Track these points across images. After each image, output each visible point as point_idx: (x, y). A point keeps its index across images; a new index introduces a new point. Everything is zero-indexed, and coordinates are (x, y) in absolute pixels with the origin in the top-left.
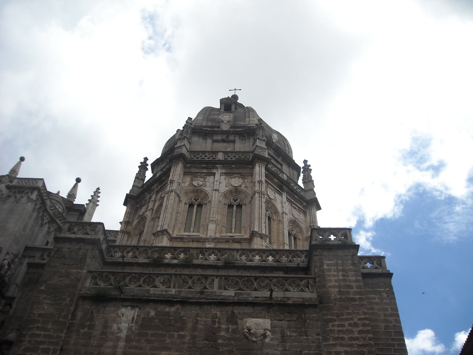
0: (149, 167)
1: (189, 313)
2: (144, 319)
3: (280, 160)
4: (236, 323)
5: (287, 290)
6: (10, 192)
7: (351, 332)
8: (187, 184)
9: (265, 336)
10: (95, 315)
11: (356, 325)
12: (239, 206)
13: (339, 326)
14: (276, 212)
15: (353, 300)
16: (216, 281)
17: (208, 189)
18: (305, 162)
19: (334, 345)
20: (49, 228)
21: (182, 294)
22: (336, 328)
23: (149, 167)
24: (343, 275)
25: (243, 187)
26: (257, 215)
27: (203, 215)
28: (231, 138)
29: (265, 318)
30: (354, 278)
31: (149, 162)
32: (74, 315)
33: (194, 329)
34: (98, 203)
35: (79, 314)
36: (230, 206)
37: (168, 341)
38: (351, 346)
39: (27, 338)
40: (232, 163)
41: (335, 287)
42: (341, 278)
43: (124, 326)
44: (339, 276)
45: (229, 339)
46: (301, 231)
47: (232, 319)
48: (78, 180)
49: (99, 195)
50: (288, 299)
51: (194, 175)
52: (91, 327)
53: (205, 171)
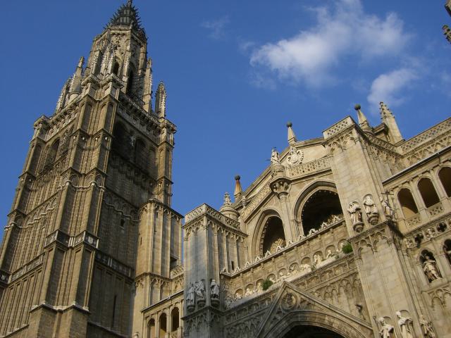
6: (330, 145)
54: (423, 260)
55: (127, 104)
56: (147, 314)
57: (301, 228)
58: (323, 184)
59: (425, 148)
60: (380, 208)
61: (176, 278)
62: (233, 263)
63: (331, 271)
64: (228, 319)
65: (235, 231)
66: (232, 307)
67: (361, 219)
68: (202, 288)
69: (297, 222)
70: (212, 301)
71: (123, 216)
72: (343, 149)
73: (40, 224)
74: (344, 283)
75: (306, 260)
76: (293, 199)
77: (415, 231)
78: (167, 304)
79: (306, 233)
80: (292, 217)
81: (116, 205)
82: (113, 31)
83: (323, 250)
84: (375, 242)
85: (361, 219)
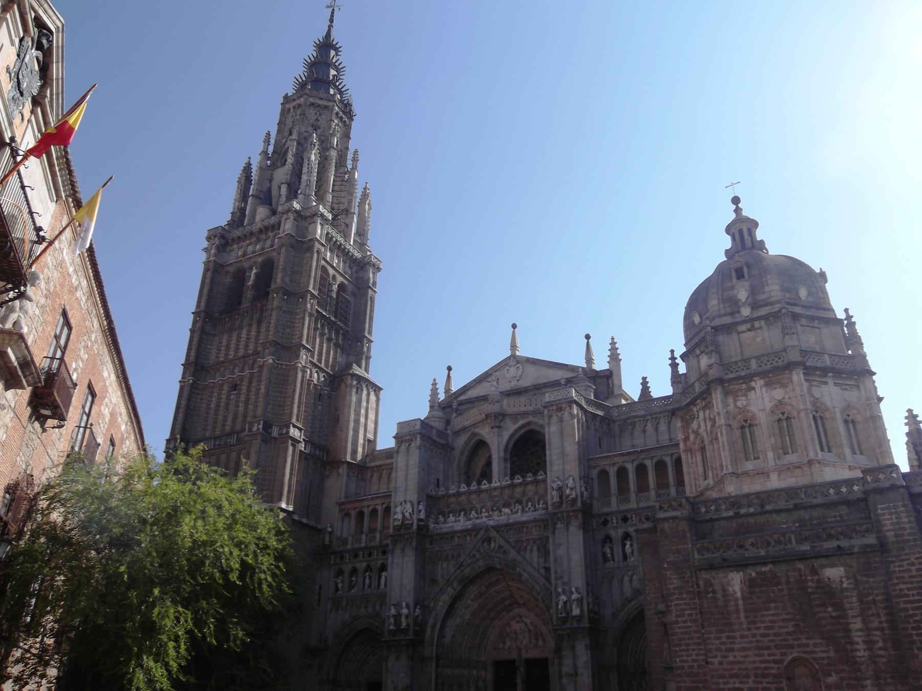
0: (679, 361)
2: (749, 580)
4: (817, 574)
5: (851, 538)
7: (910, 571)
8: (732, 407)
9: (842, 582)
10: (713, 581)
11: (913, 564)
12: (788, 418)
13: (900, 566)
15: (908, 541)
17: (754, 409)
18: (846, 310)
19: (897, 584)
20: (595, 425)
22: (897, 569)
23: (679, 361)
24: (897, 518)
25: (786, 400)
27: (758, 440)
28: (757, 324)
29: (837, 566)
30: (906, 520)
31: (677, 354)
33: (788, 583)
34: (620, 357)
35: (701, 583)
36: (779, 420)
37: (772, 595)
38: (911, 583)
39: (673, 608)
40: (769, 372)
41: (890, 530)
42: (895, 520)
43: (737, 588)
44: (892, 519)
45: (816, 588)
47: (814, 572)
48: (588, 337)
49: (617, 346)
50: (853, 546)
52: (714, 592)
53: (744, 386)
55: (332, 237)
56: (343, 507)
57: (509, 465)
58: (536, 424)
59: (637, 420)
60: (579, 494)
61: (373, 467)
62: (438, 480)
63: (528, 528)
64: (431, 543)
65: (443, 445)
68: (410, 510)
69: (505, 460)
70: (418, 525)
73: (226, 388)
76: (506, 435)
77: (604, 514)
78: (365, 503)
79: (512, 478)
80: (502, 454)
83: (525, 499)
84: (568, 524)
85: (561, 497)
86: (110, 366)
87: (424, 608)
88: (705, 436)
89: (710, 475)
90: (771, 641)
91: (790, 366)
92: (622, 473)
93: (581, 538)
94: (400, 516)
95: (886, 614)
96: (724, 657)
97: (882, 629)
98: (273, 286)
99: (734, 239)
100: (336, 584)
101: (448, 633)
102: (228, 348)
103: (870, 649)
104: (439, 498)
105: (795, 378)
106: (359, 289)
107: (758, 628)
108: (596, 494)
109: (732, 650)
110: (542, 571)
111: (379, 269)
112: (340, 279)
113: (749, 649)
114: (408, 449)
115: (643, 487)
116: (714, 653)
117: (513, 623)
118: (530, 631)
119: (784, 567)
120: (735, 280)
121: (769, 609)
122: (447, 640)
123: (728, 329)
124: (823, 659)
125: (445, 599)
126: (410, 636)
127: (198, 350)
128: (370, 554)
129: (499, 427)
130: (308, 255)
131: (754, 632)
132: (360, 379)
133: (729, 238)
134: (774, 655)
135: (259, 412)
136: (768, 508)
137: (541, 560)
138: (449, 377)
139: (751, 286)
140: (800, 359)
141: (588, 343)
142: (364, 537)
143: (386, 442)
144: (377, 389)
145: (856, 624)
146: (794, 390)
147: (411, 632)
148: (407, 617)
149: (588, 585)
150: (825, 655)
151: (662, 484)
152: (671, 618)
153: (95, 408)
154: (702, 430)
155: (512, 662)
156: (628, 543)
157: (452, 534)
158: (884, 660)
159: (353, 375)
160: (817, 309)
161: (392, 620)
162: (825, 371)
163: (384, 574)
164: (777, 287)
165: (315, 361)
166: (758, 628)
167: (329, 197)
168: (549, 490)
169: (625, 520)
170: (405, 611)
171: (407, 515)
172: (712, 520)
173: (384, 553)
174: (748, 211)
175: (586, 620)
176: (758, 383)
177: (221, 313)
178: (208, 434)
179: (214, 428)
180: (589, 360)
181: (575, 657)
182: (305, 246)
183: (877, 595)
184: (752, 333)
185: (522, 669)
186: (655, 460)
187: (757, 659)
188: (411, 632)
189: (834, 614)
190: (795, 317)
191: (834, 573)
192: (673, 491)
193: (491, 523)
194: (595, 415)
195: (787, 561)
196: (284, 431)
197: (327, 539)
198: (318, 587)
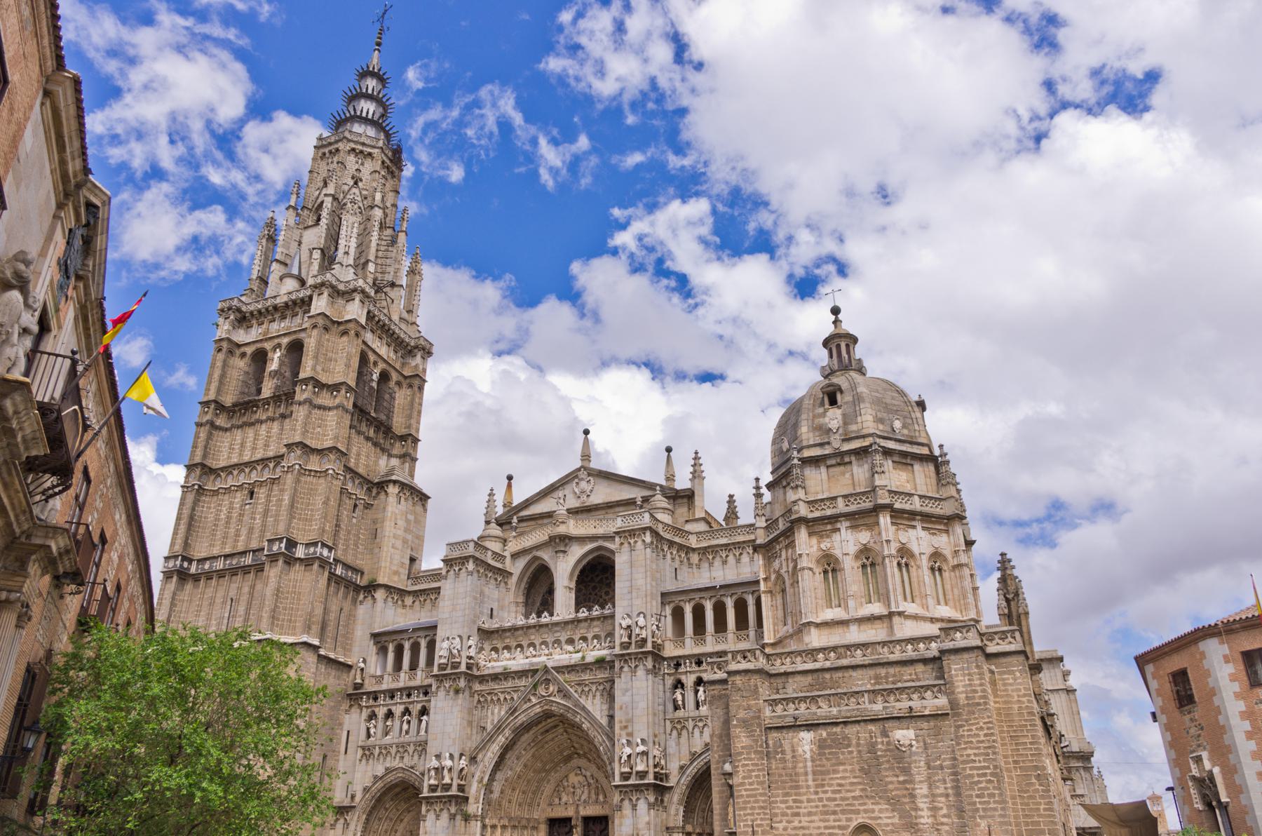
0: (764, 490)
1: (851, 730)
3: (909, 461)
7: (978, 735)
8: (815, 548)
9: (911, 746)
11: (982, 728)
12: (873, 565)
14: (912, 555)
15: (979, 704)
16: (866, 695)
17: (837, 552)
18: (941, 446)
21: (843, 714)
23: (764, 490)
25: (872, 544)
26: (891, 587)
31: (763, 483)
32: (768, 746)
33: (858, 745)
35: (770, 742)
36: (864, 566)
38: (978, 748)
39: (740, 769)
43: (807, 748)
46: (945, 560)
47: (885, 734)
51: (821, 535)
52: (783, 752)
53: (829, 527)
54: (675, 687)
56: (378, 639)
61: (416, 592)
66: (486, 672)
67: (630, 637)
71: (357, 499)
72: (632, 550)
74: (601, 688)
75: (571, 641)
78: (405, 636)
79: (577, 611)
80: (566, 583)
81: (349, 486)
82: (353, 146)
83: (590, 636)
84: (636, 666)
85: (630, 637)
86: (122, 507)
87: (473, 760)
88: (786, 576)
89: (789, 622)
90: (838, 805)
91: (877, 509)
92: (699, 613)
93: (650, 682)
94: (444, 653)
95: (953, 780)
96: (788, 822)
97: (947, 796)
98: (302, 375)
99: (831, 356)
100: (368, 729)
101: (497, 787)
102: (242, 445)
103: (934, 816)
104: (492, 632)
105: (882, 520)
106: (406, 378)
107: (826, 792)
108: (670, 633)
109: (797, 814)
110: (604, 721)
111: (430, 354)
112: (381, 366)
113: (815, 814)
114: (457, 575)
115: (721, 625)
116: (778, 819)
117: (572, 776)
118: (589, 785)
119: (856, 728)
120: (827, 406)
121: (838, 772)
122: (496, 795)
123: (815, 461)
124: (887, 825)
125: (495, 749)
126: (454, 791)
127: (206, 447)
128: (409, 695)
129: (565, 552)
130: (345, 338)
131: (821, 795)
132: (403, 486)
133: (825, 352)
134: (839, 820)
135: (281, 528)
136: (845, 662)
137: (605, 707)
138: (509, 486)
139: (844, 415)
140: (887, 501)
141: (669, 457)
142: (402, 674)
143: (431, 561)
144: (424, 498)
145: (922, 790)
146: (880, 534)
147: (455, 787)
148: (450, 770)
149: (655, 736)
150: (889, 821)
151: (742, 623)
152: (735, 781)
153: (105, 555)
154: (782, 571)
155: (569, 819)
156: (701, 689)
157: (506, 675)
158: (947, 828)
159: (395, 482)
160: (911, 443)
161: (433, 773)
162: (913, 514)
163: (425, 718)
164: (870, 418)
165: (352, 465)
166: (826, 792)
167: (371, 267)
168: (617, 628)
169: (699, 663)
170: (448, 763)
171: (455, 651)
172: (786, 674)
173: (426, 694)
174: (848, 326)
175: (651, 776)
176: (843, 525)
177: (234, 405)
178: (216, 552)
179: (224, 543)
180: (670, 478)
181: (635, 816)
182: (342, 328)
183: (944, 760)
184: (842, 468)
185: (579, 829)
186: (735, 597)
187: (822, 824)
188: (455, 787)
189: (901, 779)
190: (887, 453)
191: (904, 735)
192: (752, 633)
193: (550, 664)
194: (671, 544)
195: (858, 722)
196: (312, 550)
197: (358, 676)
198: (345, 733)
